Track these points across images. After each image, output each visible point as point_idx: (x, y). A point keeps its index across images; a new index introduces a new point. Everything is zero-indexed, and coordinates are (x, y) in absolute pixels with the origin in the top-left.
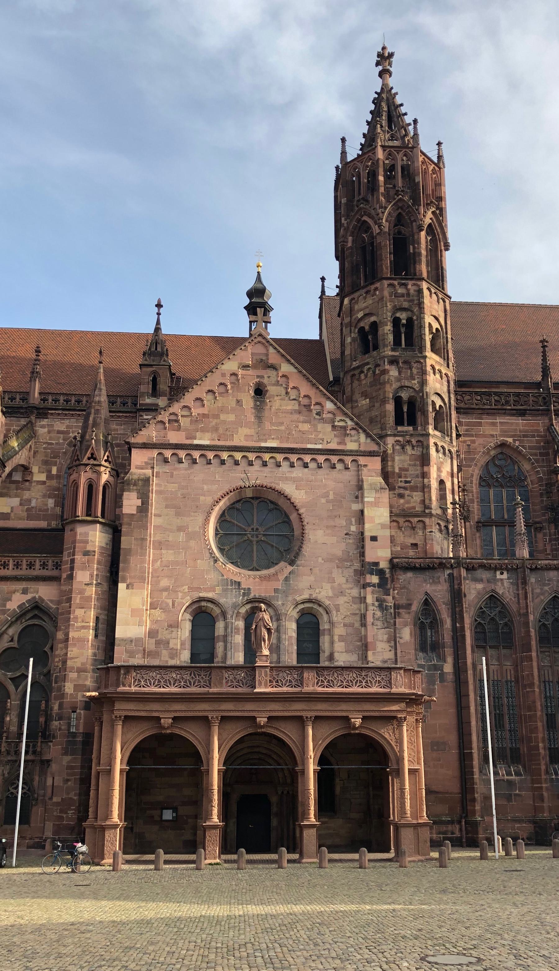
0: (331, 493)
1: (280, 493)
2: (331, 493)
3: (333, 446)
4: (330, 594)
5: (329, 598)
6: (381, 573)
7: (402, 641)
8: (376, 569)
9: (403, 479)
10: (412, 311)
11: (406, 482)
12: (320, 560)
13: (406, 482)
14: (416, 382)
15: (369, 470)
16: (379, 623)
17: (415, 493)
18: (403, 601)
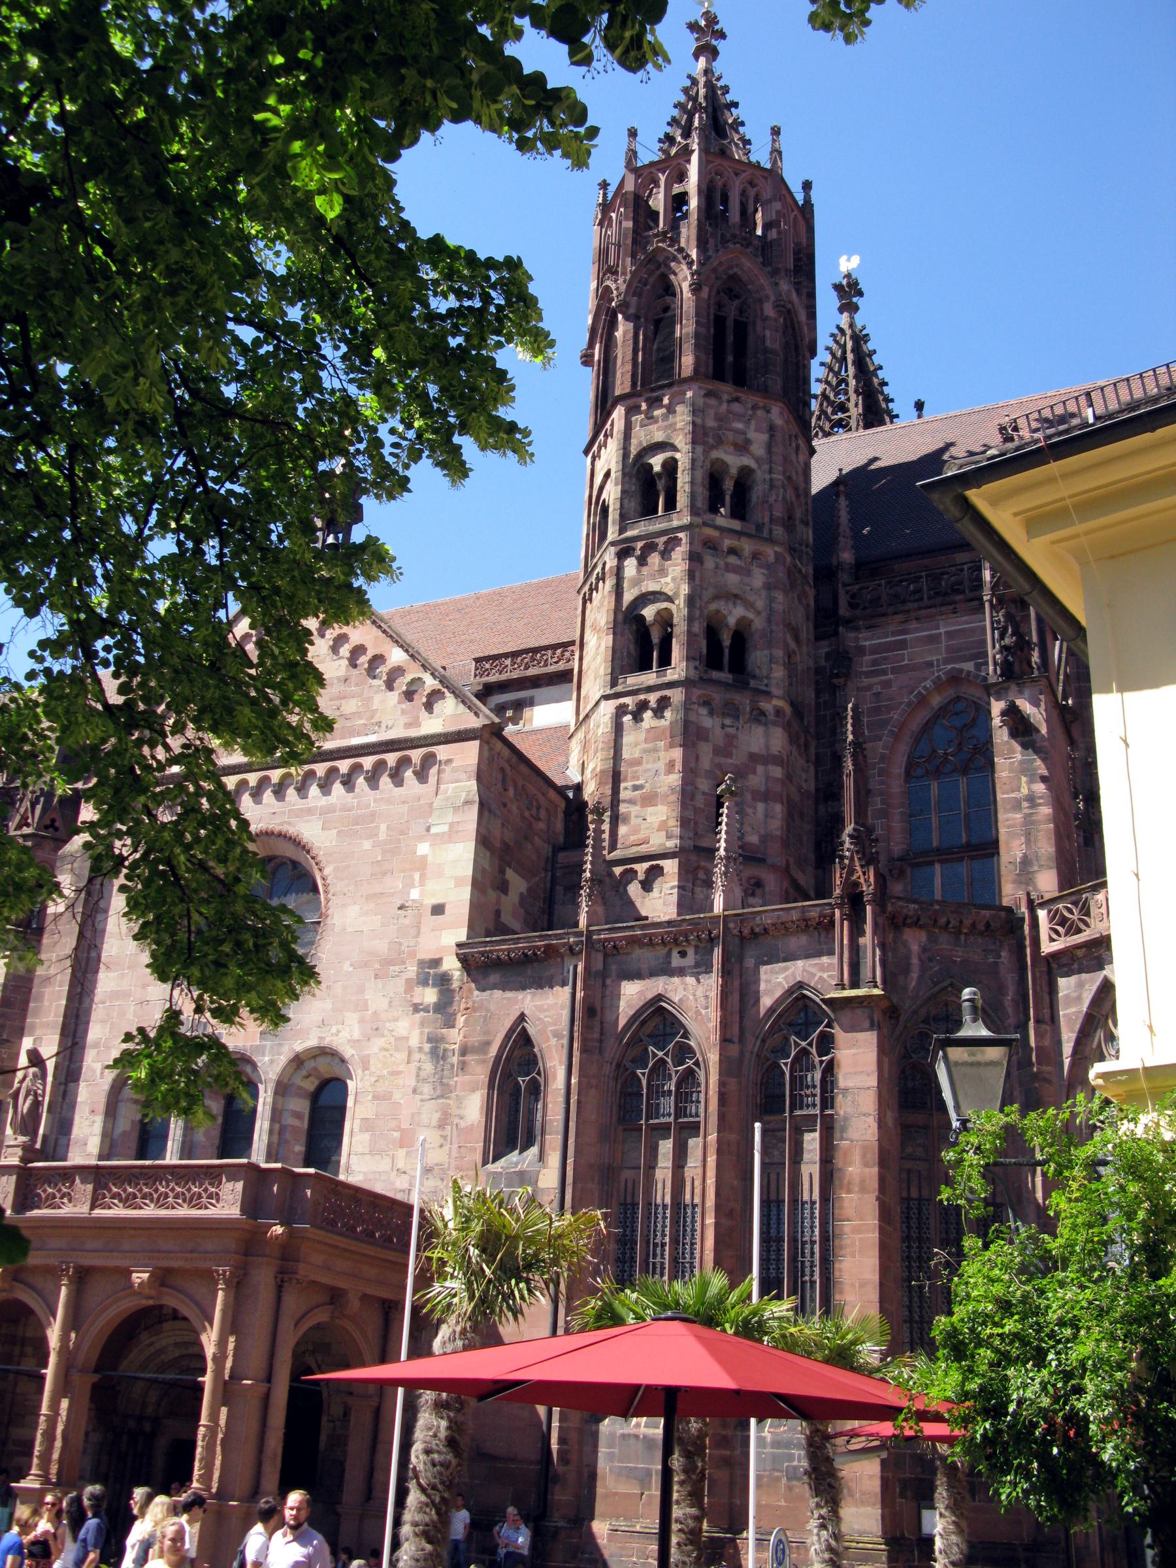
0: (383, 827)
1: (296, 842)
2: (383, 827)
3: (398, 732)
4: (356, 1035)
5: (353, 1043)
6: (443, 980)
7: (463, 1124)
8: (436, 975)
9: (629, 784)
10: (674, 448)
11: (636, 788)
12: (347, 967)
13: (636, 788)
14: (668, 579)
15: (455, 770)
16: (427, 1089)
17: (650, 809)
18: (475, 1039)
